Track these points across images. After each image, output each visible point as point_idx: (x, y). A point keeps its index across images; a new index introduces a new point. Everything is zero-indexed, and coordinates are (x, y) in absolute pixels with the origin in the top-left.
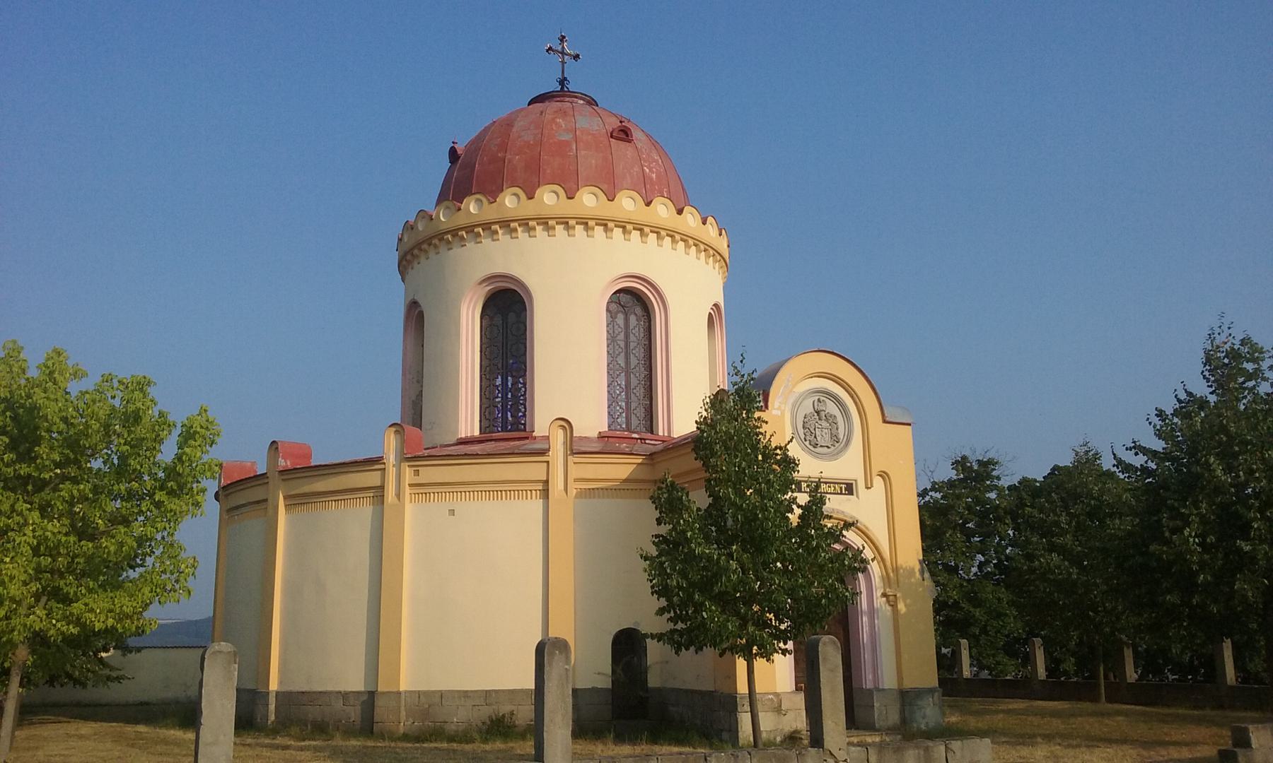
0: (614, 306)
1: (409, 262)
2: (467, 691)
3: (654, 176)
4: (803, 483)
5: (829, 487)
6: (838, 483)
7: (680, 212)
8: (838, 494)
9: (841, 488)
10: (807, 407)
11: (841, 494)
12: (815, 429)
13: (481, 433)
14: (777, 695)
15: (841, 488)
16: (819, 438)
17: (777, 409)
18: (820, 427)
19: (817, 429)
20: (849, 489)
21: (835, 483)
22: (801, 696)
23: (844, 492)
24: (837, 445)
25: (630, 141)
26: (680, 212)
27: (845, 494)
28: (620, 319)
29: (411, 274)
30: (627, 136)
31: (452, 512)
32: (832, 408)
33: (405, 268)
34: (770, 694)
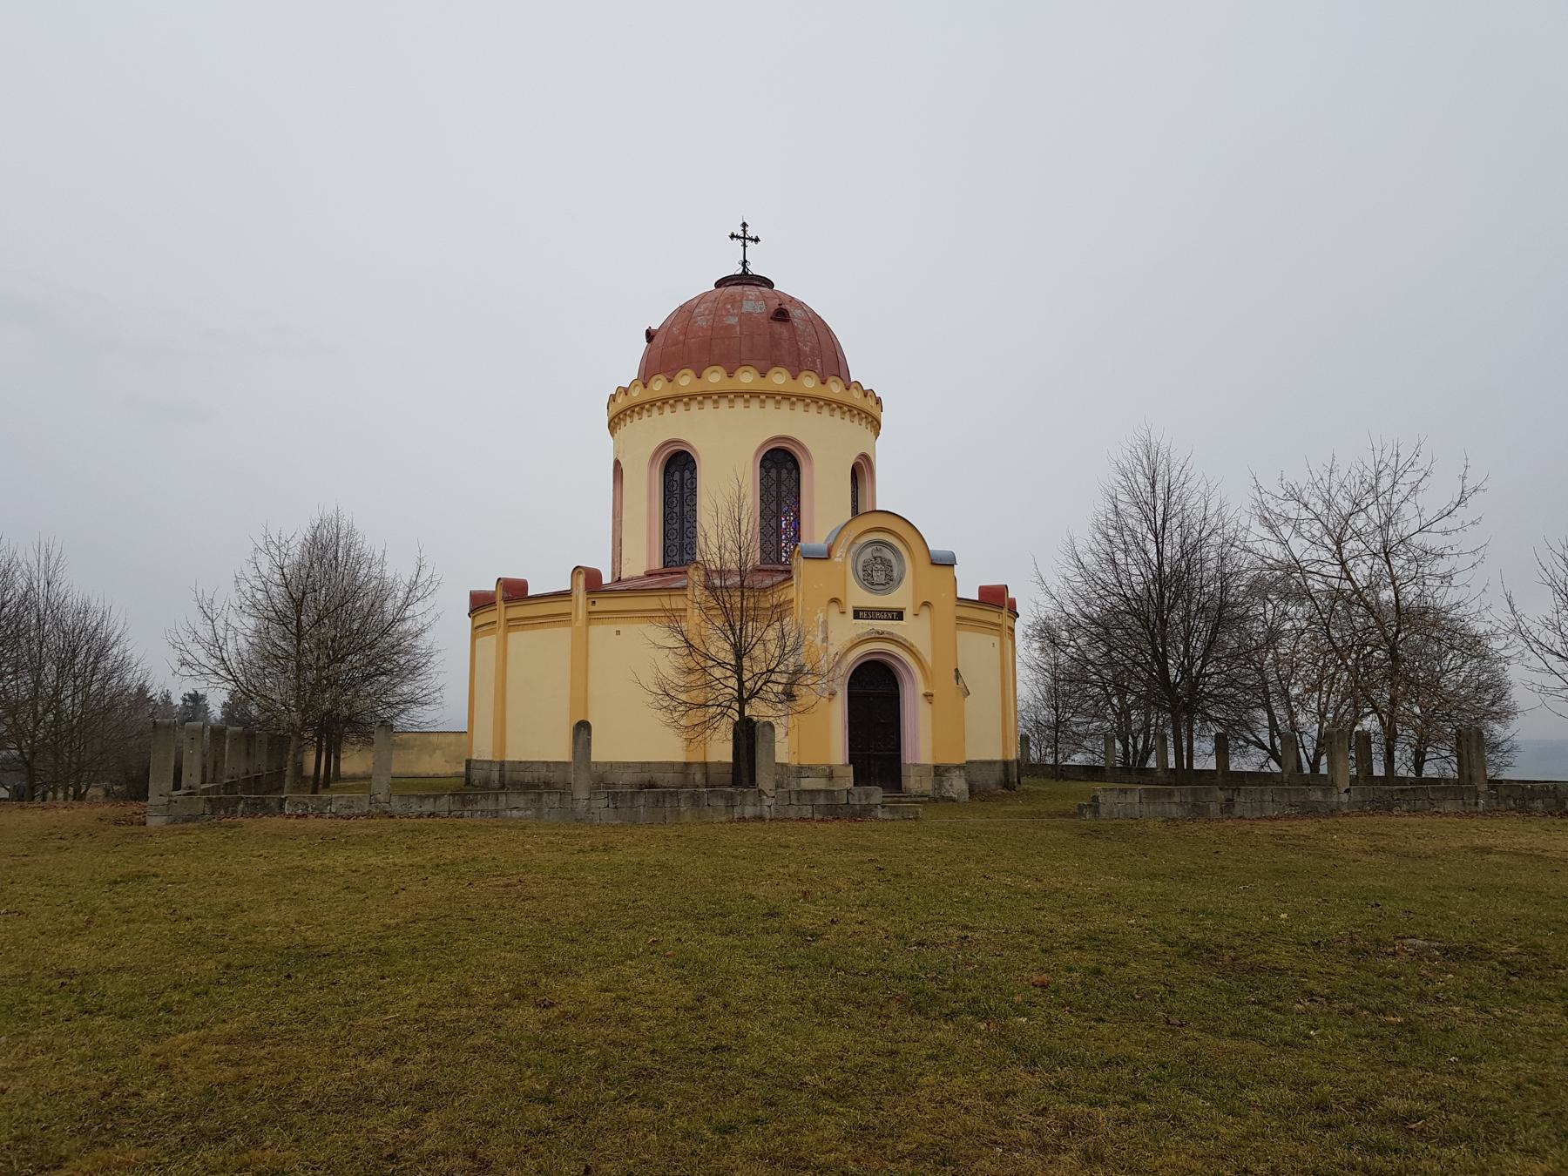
0: (768, 464)
1: (617, 424)
2: (628, 763)
3: (807, 349)
7: (823, 383)
10: (867, 554)
11: (893, 619)
13: (664, 567)
14: (830, 767)
16: (875, 578)
20: (899, 615)
22: (852, 767)
24: (891, 583)
25: (788, 320)
26: (823, 383)
27: (896, 620)
28: (773, 473)
29: (623, 431)
31: (618, 632)
32: (887, 554)
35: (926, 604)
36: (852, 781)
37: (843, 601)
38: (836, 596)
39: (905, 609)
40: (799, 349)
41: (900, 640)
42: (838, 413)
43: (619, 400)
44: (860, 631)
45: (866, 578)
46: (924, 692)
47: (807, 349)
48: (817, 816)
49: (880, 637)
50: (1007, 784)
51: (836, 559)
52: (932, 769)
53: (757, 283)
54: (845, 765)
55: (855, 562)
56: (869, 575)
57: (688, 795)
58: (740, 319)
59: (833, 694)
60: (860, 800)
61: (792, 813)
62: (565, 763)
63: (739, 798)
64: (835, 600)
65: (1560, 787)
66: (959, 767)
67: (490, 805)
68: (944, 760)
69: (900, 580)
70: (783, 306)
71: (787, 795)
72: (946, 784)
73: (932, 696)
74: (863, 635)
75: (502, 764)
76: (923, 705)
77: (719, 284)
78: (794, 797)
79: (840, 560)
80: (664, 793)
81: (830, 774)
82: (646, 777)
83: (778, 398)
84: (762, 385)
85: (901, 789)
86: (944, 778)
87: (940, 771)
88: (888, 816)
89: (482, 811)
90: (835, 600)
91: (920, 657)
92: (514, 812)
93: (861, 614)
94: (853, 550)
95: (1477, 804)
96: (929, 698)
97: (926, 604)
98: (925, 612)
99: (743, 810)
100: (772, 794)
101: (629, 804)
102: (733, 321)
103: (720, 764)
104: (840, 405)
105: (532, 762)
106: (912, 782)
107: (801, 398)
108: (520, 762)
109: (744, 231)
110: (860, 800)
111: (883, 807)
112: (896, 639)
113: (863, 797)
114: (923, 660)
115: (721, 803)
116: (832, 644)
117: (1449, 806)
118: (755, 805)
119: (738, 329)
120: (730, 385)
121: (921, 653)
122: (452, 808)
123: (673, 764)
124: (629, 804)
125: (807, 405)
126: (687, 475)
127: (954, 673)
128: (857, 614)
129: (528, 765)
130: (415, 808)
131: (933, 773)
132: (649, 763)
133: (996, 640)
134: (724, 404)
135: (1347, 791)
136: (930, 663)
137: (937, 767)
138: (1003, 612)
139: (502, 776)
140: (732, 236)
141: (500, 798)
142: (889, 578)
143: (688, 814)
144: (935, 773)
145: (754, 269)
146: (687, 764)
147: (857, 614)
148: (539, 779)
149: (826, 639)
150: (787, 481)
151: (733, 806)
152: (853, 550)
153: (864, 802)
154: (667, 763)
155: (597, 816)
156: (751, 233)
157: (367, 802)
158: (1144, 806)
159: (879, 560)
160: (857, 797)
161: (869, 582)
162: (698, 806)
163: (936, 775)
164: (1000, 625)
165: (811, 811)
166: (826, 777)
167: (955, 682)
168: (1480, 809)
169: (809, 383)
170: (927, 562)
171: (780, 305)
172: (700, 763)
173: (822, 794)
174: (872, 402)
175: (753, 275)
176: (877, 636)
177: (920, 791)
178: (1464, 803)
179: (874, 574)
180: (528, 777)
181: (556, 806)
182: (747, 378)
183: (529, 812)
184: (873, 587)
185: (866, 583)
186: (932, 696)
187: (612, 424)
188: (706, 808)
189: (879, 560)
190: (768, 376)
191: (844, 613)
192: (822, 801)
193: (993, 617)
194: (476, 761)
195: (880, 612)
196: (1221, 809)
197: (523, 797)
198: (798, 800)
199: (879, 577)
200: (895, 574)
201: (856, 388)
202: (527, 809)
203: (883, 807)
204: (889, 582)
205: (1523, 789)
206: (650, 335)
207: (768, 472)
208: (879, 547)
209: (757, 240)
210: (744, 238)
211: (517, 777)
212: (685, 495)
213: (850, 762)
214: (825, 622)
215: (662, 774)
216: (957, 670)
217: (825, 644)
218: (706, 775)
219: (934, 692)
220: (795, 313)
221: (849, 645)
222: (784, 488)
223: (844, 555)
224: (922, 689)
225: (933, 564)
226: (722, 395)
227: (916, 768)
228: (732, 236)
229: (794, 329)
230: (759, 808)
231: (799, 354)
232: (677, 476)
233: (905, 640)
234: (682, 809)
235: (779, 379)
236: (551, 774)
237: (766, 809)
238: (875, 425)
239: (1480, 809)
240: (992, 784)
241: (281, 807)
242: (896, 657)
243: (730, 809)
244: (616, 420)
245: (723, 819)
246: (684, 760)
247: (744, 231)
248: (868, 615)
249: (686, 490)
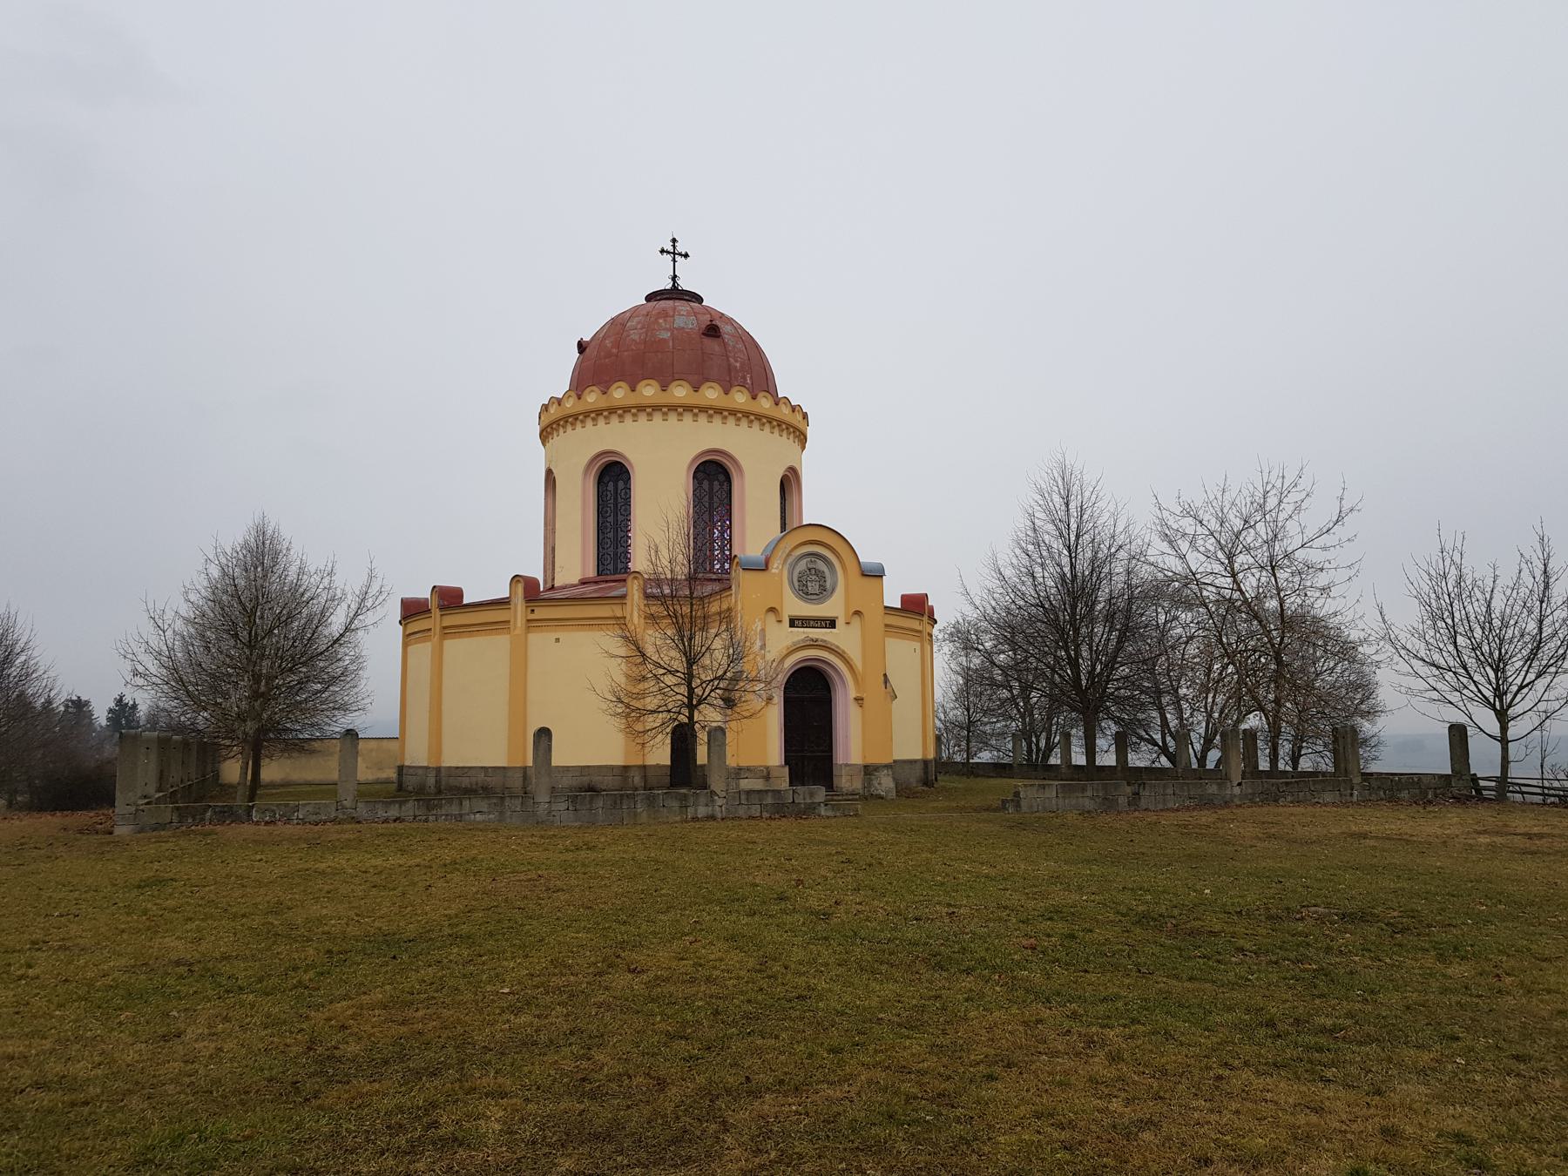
0: (700, 475)
3: (738, 365)
6: (823, 620)
7: (754, 398)
10: (802, 565)
11: (826, 627)
13: (598, 575)
14: (767, 768)
20: (831, 623)
22: (787, 769)
24: (825, 593)
25: (719, 337)
26: (754, 398)
28: (706, 484)
30: (716, 332)
32: (821, 566)
33: (547, 437)
34: (761, 766)
35: (857, 613)
36: (788, 780)
37: (779, 610)
38: (773, 606)
39: (837, 618)
40: (729, 365)
41: (833, 647)
42: (767, 428)
43: (552, 410)
44: (796, 639)
46: (854, 696)
47: (738, 365)
48: (765, 815)
49: (814, 644)
50: (926, 782)
51: (773, 571)
52: (862, 769)
53: (687, 298)
54: (781, 766)
55: (791, 573)
57: (644, 797)
58: (672, 334)
59: (770, 699)
60: (804, 799)
61: (741, 811)
62: (504, 768)
63: (692, 800)
64: (772, 610)
65: (1424, 779)
66: (887, 766)
67: (455, 810)
68: (874, 760)
69: (833, 590)
70: (714, 323)
71: (737, 795)
72: (875, 783)
73: (862, 699)
74: (799, 642)
75: (438, 769)
76: (854, 709)
77: (649, 298)
78: (743, 797)
79: (777, 571)
80: (622, 795)
81: (767, 775)
82: (586, 780)
83: (711, 412)
84: (694, 399)
85: (832, 788)
86: (873, 777)
87: (869, 770)
88: (830, 813)
89: (447, 815)
90: (772, 610)
91: (852, 663)
92: (478, 815)
93: (796, 622)
94: (789, 561)
95: (1351, 795)
96: (860, 702)
97: (857, 613)
98: (856, 621)
99: (696, 810)
100: (724, 794)
101: (588, 806)
102: (666, 335)
103: (658, 766)
104: (770, 420)
105: (470, 768)
106: (844, 782)
107: (733, 412)
108: (457, 768)
109: (674, 247)
110: (804, 799)
111: (826, 805)
112: (829, 646)
113: (807, 796)
114: (854, 666)
115: (675, 804)
116: (769, 652)
117: (1328, 797)
118: (707, 805)
119: (671, 344)
120: (663, 399)
121: (852, 660)
122: (417, 813)
123: (612, 768)
124: (588, 806)
125: (739, 419)
126: (621, 485)
127: (883, 678)
128: (793, 622)
129: (466, 770)
130: (381, 813)
131: (863, 773)
132: (589, 767)
133: (917, 645)
134: (658, 417)
135: (1239, 784)
136: (861, 670)
137: (866, 767)
138: (924, 619)
139: (438, 782)
140: (662, 251)
141: (464, 803)
142: (823, 589)
143: (645, 815)
144: (865, 772)
145: (684, 284)
146: (626, 768)
147: (793, 622)
148: (477, 784)
149: (763, 646)
150: (719, 492)
151: (686, 807)
152: (789, 561)
153: (808, 801)
154: (606, 766)
155: (558, 818)
156: (679, 249)
157: (334, 809)
158: (1061, 801)
160: (801, 797)
161: (804, 592)
162: (654, 807)
163: (866, 774)
164: (920, 632)
165: (759, 810)
166: (763, 777)
167: (883, 686)
168: (1355, 799)
169: (740, 398)
170: (854, 571)
171: (711, 321)
172: (639, 767)
173: (770, 794)
174: (800, 418)
175: (683, 290)
176: (812, 643)
177: (850, 789)
178: (1341, 795)
179: (809, 584)
180: (465, 782)
181: (518, 809)
182: (680, 392)
183: (491, 816)
184: (809, 597)
185: (801, 592)
186: (862, 699)
187: (544, 433)
188: (661, 809)
189: (813, 572)
190: (700, 390)
191: (780, 621)
192: (769, 800)
193: (915, 624)
194: (409, 767)
195: (814, 620)
196: (1129, 801)
197: (486, 801)
198: (747, 799)
199: (813, 587)
200: (828, 585)
201: (784, 403)
202: (489, 813)
203: (826, 805)
204: (823, 593)
205: (1392, 781)
206: (581, 346)
207: (700, 483)
208: (813, 559)
209: (686, 256)
210: (674, 253)
211: (453, 782)
212: (619, 505)
213: (787, 762)
214: (763, 630)
215: (600, 778)
216: (885, 675)
217: (763, 652)
218: (645, 777)
219: (864, 696)
220: (725, 329)
221: (785, 652)
222: (715, 499)
223: (780, 567)
224: (853, 694)
225: (864, 575)
226: (656, 408)
227: (848, 768)
228: (662, 251)
229: (725, 345)
230: (710, 809)
231: (729, 370)
232: (611, 486)
233: (838, 647)
234: (639, 810)
235: (711, 394)
236: (489, 779)
237: (718, 809)
238: (802, 438)
239: (1355, 799)
240: (913, 781)
241: (249, 815)
242: (829, 664)
243: (684, 809)
244: (549, 430)
245: (678, 819)
246: (620, 762)
247: (674, 247)
249: (619, 500)
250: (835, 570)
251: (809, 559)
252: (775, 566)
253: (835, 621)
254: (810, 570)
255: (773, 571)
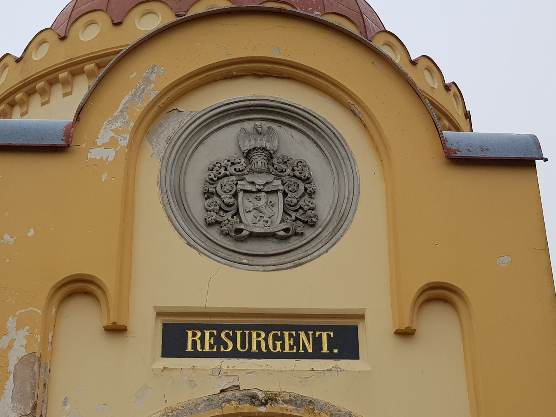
4: (190, 333)
5: (276, 338)
8: (306, 356)
9: (317, 342)
11: (317, 354)
12: (235, 195)
15: (317, 342)
17: (107, 146)
18: (249, 187)
19: (241, 195)
21: (298, 328)
23: (325, 349)
27: (330, 356)
45: (214, 216)
56: (224, 208)
79: (111, 154)
159: (259, 161)
179: (244, 202)
185: (214, 233)
189: (259, 161)
195: (267, 329)
208: (266, 125)
223: (124, 141)
248: (219, 341)
250: (349, 156)
251: (249, 126)
252: (104, 136)
253: (355, 329)
254: (248, 155)
255: (95, 154)
